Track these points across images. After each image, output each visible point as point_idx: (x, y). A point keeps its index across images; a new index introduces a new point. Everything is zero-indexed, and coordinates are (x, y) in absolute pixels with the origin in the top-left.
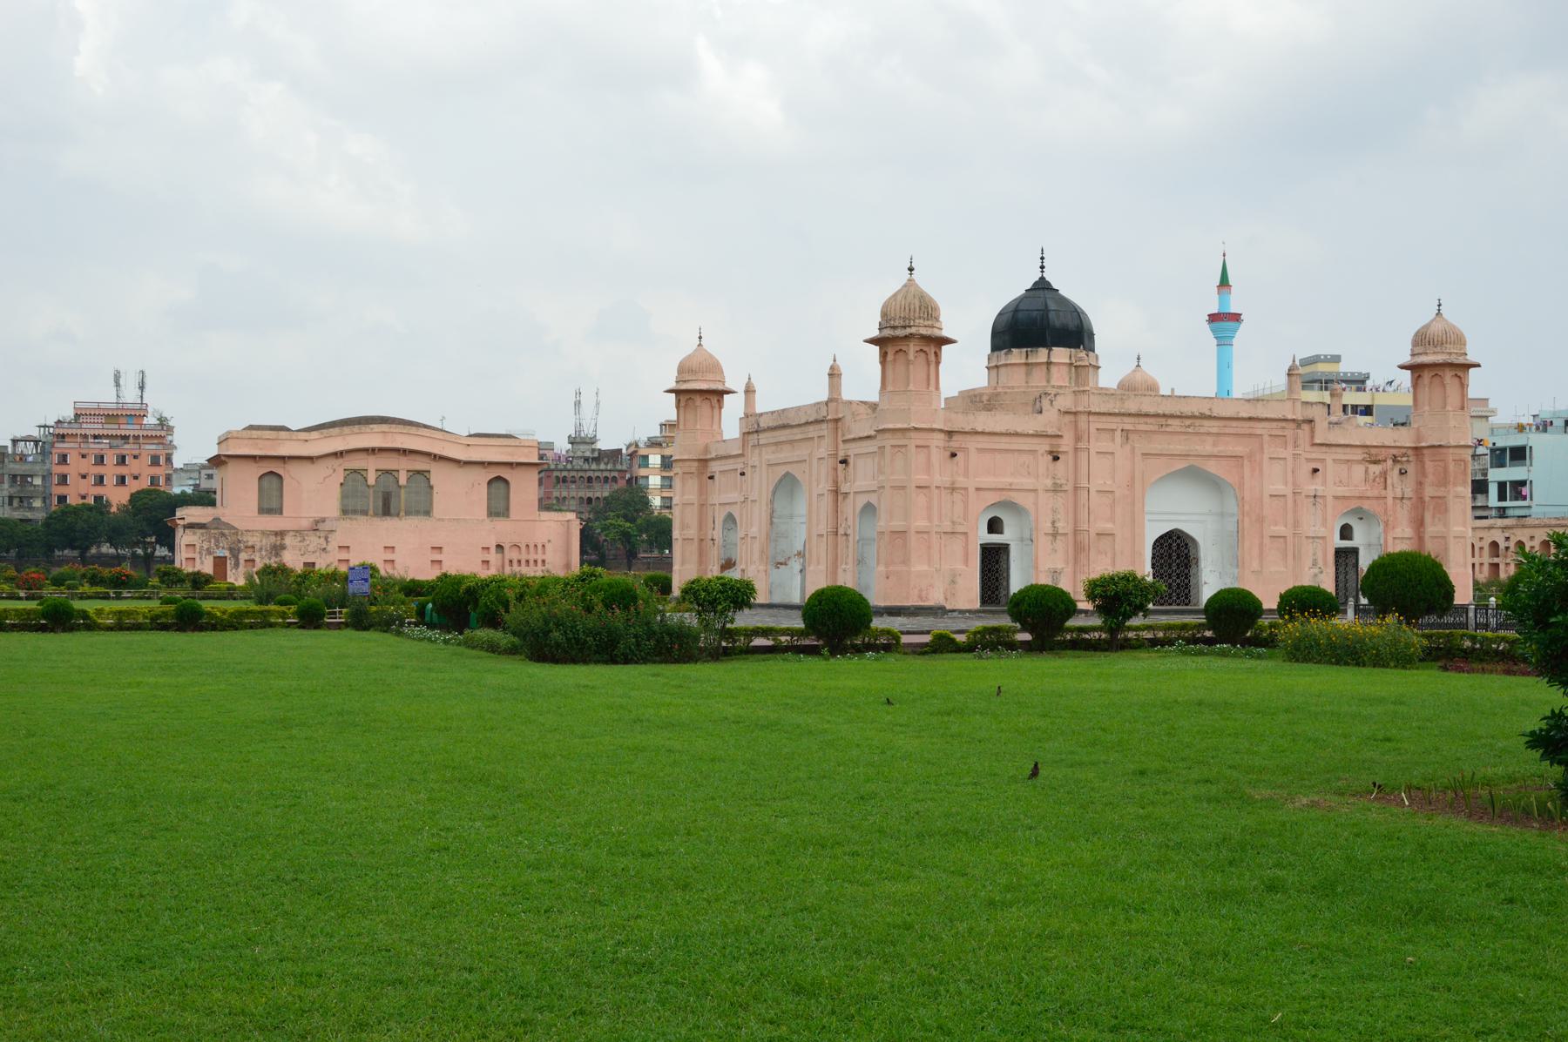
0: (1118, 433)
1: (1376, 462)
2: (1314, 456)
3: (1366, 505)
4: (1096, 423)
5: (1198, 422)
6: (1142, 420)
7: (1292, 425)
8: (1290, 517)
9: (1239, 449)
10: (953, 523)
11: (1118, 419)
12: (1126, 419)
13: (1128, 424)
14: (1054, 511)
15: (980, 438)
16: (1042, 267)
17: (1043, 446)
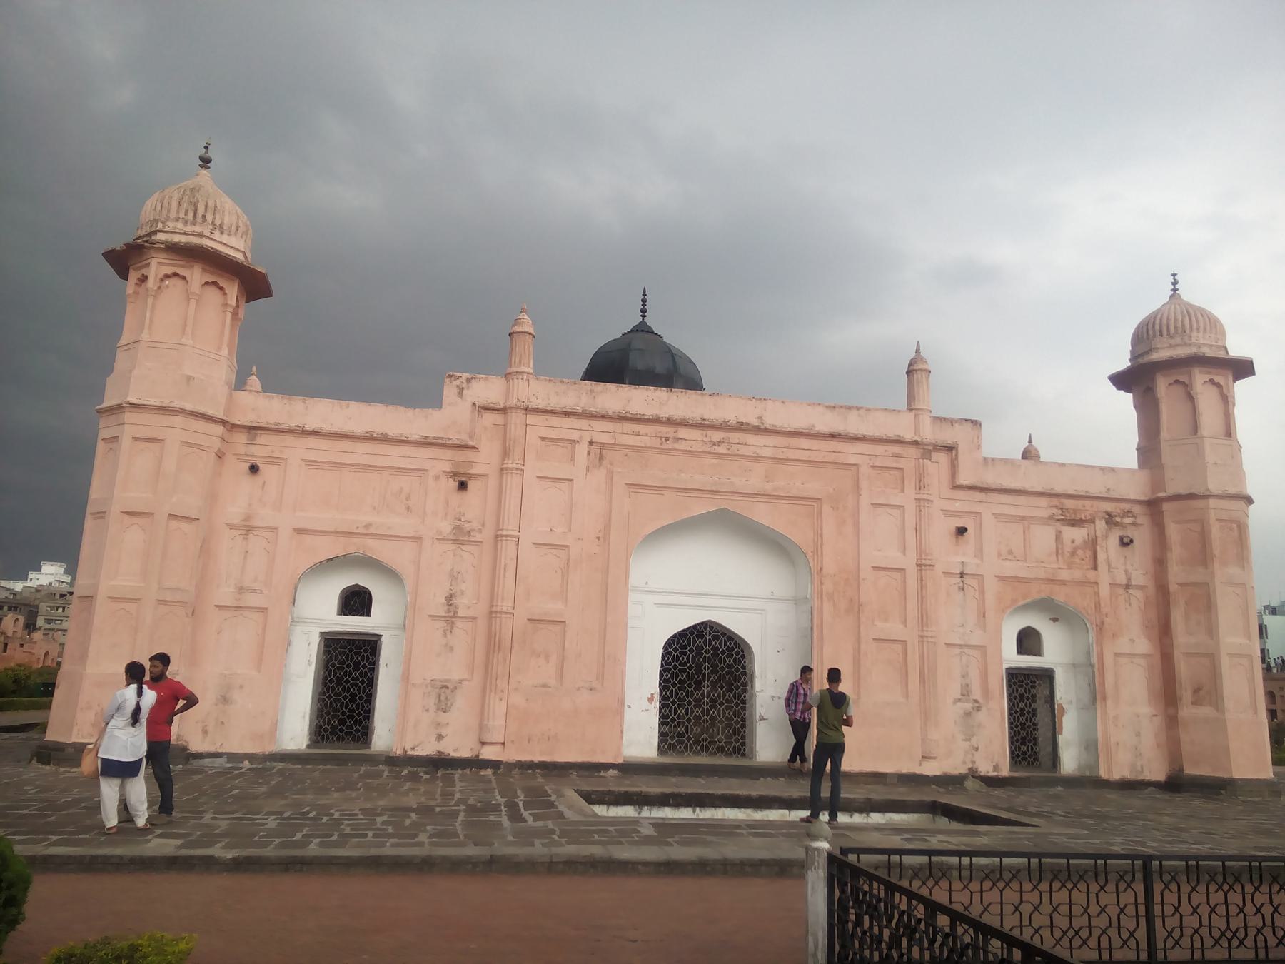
0: (582, 449)
1: (1075, 523)
2: (958, 506)
3: (1060, 596)
4: (538, 427)
5: (735, 437)
6: (629, 427)
7: (913, 451)
8: (912, 605)
9: (813, 485)
10: (241, 589)
11: (583, 423)
12: (598, 425)
13: (603, 432)
14: (454, 577)
15: (312, 442)
16: (644, 311)
17: (442, 461)
